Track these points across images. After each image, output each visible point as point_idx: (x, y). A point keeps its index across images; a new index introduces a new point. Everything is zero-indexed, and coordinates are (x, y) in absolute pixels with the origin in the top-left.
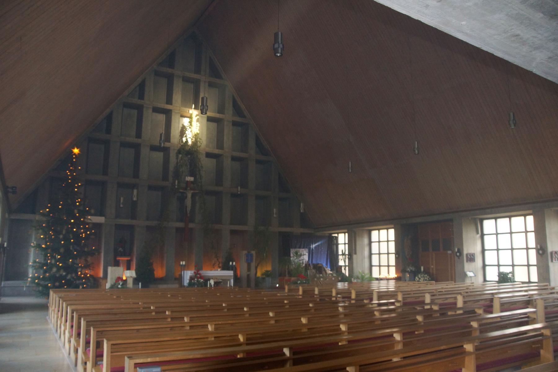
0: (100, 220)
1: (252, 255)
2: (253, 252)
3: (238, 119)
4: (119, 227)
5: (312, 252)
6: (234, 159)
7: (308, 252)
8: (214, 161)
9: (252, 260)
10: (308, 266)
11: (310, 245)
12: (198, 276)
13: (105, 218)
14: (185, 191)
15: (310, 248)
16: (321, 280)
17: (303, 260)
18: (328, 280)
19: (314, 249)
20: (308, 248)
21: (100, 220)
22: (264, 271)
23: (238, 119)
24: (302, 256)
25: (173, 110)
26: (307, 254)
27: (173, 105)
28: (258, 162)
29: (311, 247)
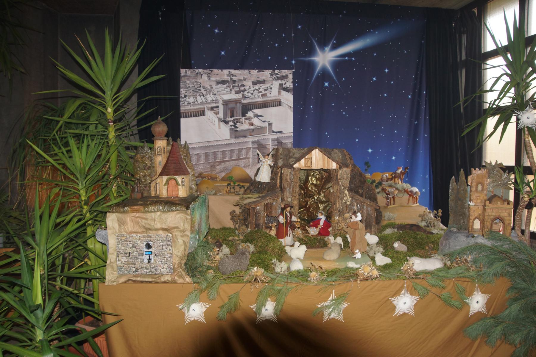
17: (260, 130)
24: (258, 111)
26: (288, 98)
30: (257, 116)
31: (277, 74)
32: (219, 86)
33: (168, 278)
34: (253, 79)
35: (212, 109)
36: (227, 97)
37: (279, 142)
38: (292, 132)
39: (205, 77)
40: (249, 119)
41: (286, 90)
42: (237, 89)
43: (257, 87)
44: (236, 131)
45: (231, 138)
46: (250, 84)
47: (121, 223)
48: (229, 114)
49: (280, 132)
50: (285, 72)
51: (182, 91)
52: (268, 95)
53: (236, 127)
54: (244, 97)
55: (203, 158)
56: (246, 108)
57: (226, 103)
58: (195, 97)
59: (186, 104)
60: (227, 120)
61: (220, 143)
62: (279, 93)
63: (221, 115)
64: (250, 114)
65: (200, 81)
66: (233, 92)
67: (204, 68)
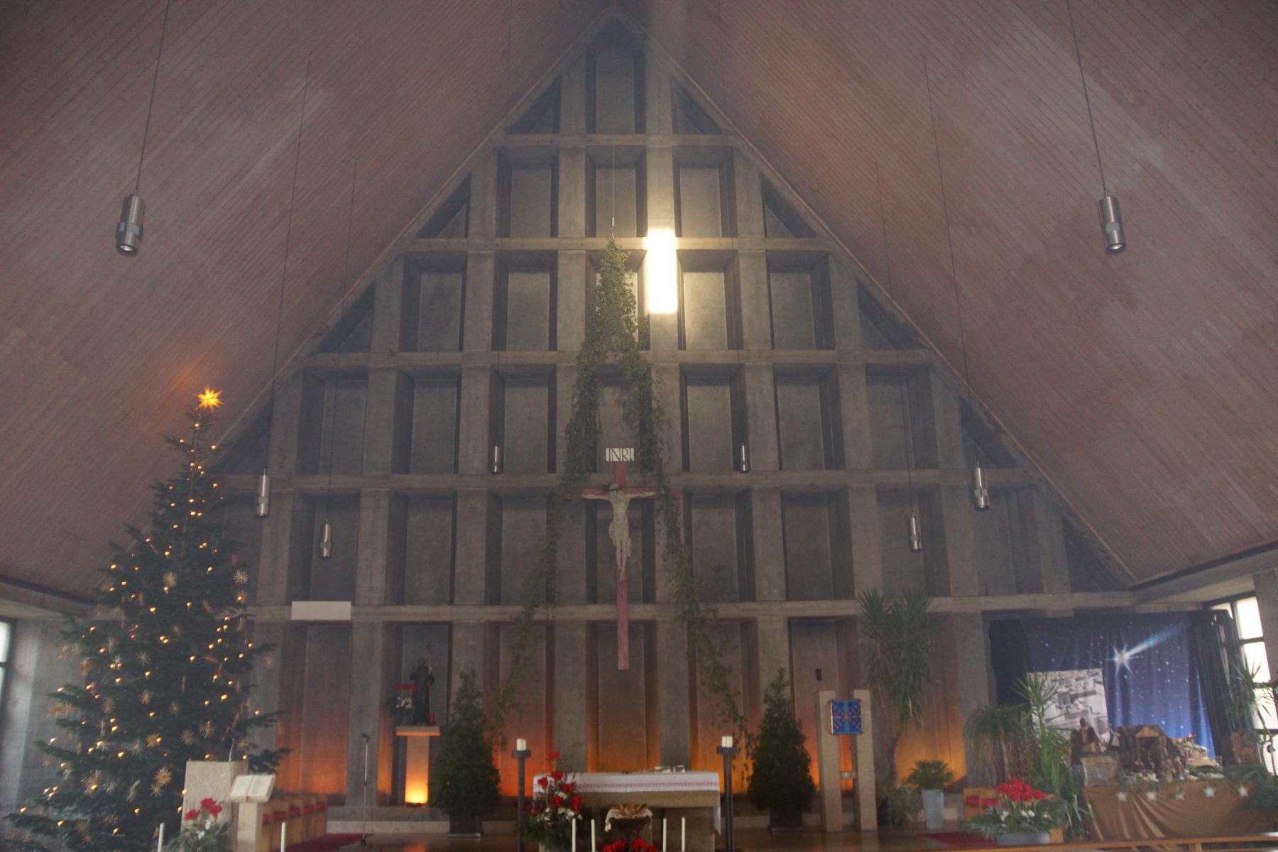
0: (339, 610)
1: (855, 707)
2: (863, 695)
3: (788, 244)
4: (397, 630)
5: (1123, 681)
6: (782, 376)
7: (1104, 683)
8: (725, 392)
9: (856, 725)
10: (1084, 736)
11: (1112, 655)
12: (561, 794)
13: (353, 604)
14: (605, 497)
15: (1112, 664)
16: (1146, 798)
17: (1085, 712)
19: (1127, 666)
20: (1104, 666)
21: (339, 610)
22: (914, 766)
23: (788, 244)
24: (1081, 699)
25: (559, 252)
26: (1101, 689)
27: (559, 236)
28: (874, 374)
29: (1117, 659)
30: (1081, 703)
34: (1076, 677)
38: (1106, 714)
40: (1076, 705)
41: (1099, 683)
43: (1079, 682)
47: (1088, 762)
49: (1098, 713)
52: (1087, 687)
62: (1094, 686)
64: (1076, 702)
66: (1063, 687)
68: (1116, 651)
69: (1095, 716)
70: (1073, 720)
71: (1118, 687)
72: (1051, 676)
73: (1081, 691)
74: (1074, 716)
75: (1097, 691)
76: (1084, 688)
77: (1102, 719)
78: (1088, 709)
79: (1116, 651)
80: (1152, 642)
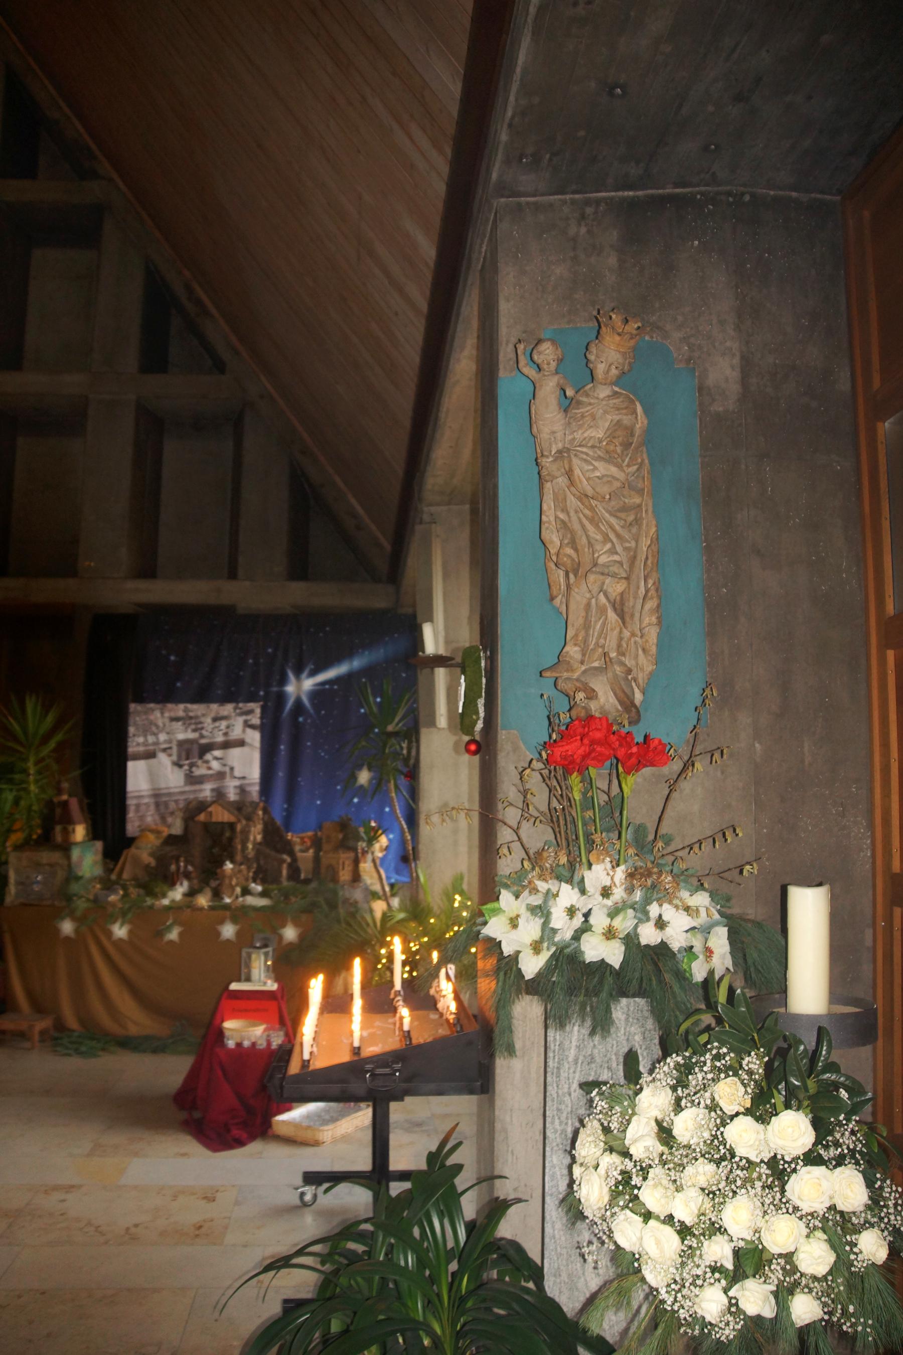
5: (296, 725)
7: (262, 728)
11: (283, 681)
15: (281, 697)
16: (109, 934)
17: (221, 775)
18: (173, 935)
19: (305, 700)
20: (265, 699)
24: (217, 753)
26: (254, 737)
29: (290, 688)
30: (216, 758)
31: (240, 709)
32: (174, 723)
33: (49, 902)
34: (213, 715)
35: (164, 750)
36: (181, 736)
37: (242, 790)
39: (158, 714)
40: (207, 762)
41: (253, 727)
42: (193, 727)
43: (217, 724)
44: (192, 777)
45: (186, 784)
46: (209, 720)
48: (184, 755)
49: (244, 778)
50: (251, 705)
51: (132, 730)
52: (231, 734)
53: (192, 772)
54: (202, 736)
55: (152, 808)
56: (206, 749)
57: (181, 743)
58: (145, 736)
59: (134, 744)
60: (182, 763)
61: (172, 791)
62: (244, 731)
63: (175, 758)
64: (208, 757)
65: (152, 717)
66: (189, 730)
67: (157, 702)
68: (291, 676)
69: (237, 783)
70: (197, 787)
71: (285, 736)
72: (170, 711)
73: (220, 739)
74: (200, 780)
75: (248, 740)
76: (226, 734)
77: (248, 789)
78: (227, 769)
79: (291, 676)
80: (357, 663)
